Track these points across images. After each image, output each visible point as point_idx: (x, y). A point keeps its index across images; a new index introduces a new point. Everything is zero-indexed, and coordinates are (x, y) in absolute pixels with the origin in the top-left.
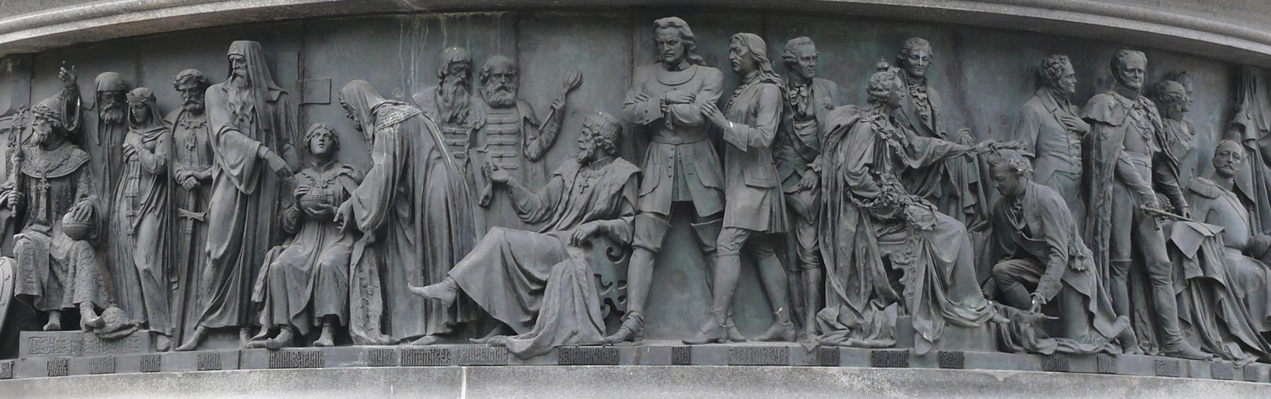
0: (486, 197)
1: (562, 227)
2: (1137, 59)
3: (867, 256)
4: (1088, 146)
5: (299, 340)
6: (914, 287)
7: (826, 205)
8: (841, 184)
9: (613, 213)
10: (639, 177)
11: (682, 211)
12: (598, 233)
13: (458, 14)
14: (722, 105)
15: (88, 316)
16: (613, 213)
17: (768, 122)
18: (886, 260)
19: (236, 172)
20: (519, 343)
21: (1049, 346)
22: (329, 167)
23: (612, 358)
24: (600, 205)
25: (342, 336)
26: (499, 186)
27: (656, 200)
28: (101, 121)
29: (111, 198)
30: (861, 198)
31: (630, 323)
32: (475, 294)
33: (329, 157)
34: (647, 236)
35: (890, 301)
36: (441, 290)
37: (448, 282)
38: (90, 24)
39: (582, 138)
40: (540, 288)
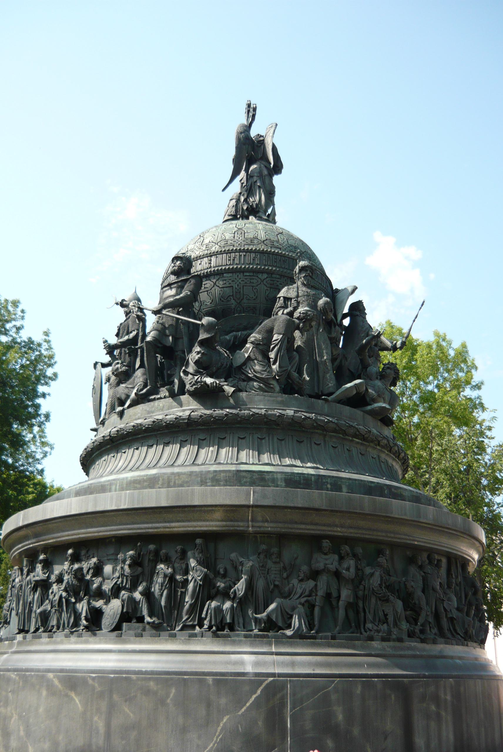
0: (272, 589)
1: (295, 598)
3: (378, 610)
4: (425, 579)
5: (218, 629)
6: (391, 619)
7: (366, 595)
8: (371, 589)
9: (309, 596)
10: (316, 585)
11: (328, 596)
12: (306, 601)
13: (263, 535)
15: (148, 619)
16: (309, 596)
17: (352, 570)
18: (383, 611)
19: (199, 578)
22: (225, 578)
24: (307, 593)
26: (276, 586)
27: (321, 593)
28: (149, 559)
29: (150, 582)
30: (377, 593)
31: (316, 627)
34: (318, 601)
35: (384, 623)
37: (265, 614)
38: (150, 530)
39: (299, 573)
40: (291, 617)
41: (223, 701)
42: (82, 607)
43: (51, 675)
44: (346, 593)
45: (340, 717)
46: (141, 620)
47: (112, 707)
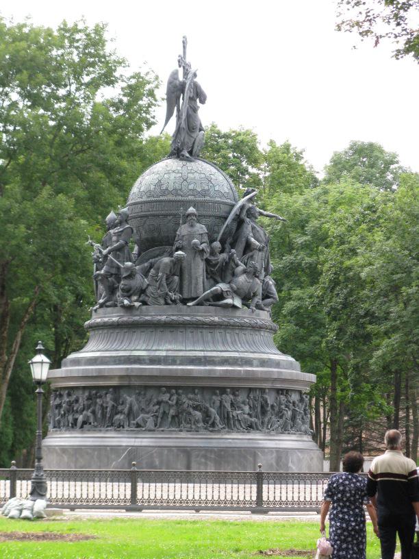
2: (229, 390)
4: (221, 402)
5: (118, 428)
10: (159, 408)
11: (164, 412)
14: (170, 399)
15: (92, 424)
17: (175, 402)
20: (144, 429)
21: (211, 429)
23: (154, 431)
25: (123, 427)
27: (161, 411)
32: (139, 422)
33: (122, 404)
34: (160, 416)
36: (135, 422)
41: (113, 456)
42: (70, 418)
43: (57, 448)
44: (172, 412)
45: (157, 463)
46: (90, 424)
47: (77, 459)
